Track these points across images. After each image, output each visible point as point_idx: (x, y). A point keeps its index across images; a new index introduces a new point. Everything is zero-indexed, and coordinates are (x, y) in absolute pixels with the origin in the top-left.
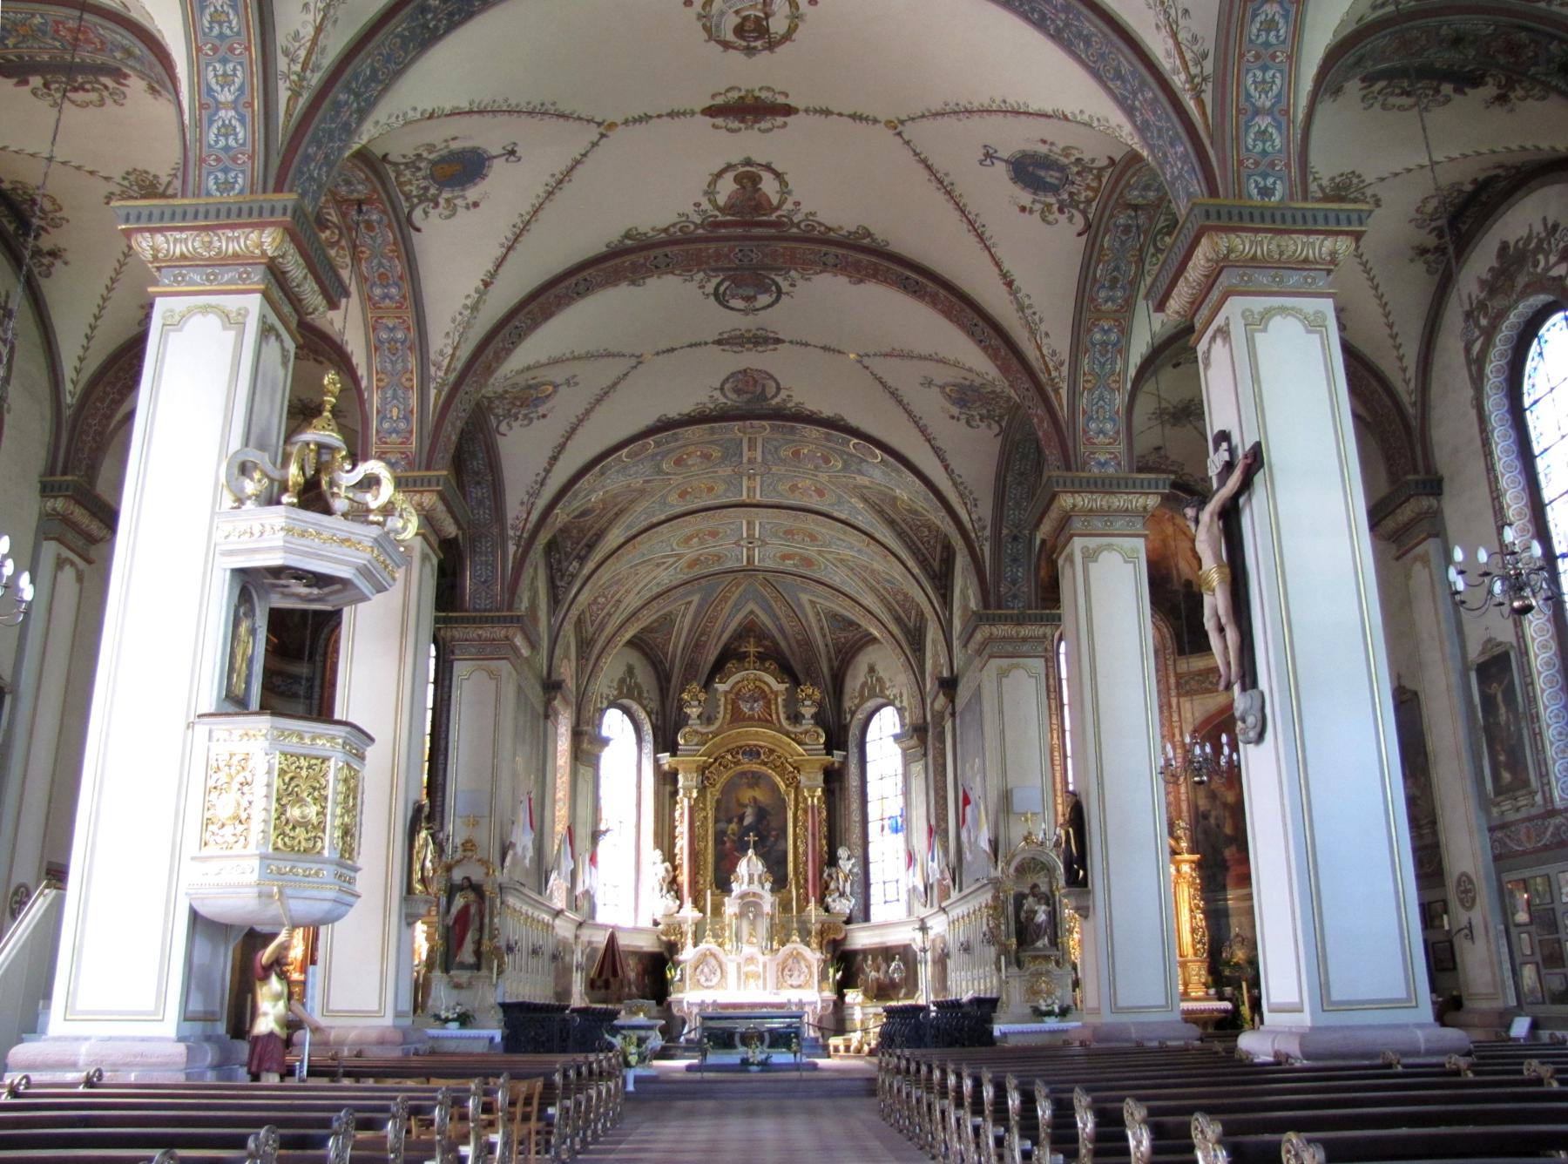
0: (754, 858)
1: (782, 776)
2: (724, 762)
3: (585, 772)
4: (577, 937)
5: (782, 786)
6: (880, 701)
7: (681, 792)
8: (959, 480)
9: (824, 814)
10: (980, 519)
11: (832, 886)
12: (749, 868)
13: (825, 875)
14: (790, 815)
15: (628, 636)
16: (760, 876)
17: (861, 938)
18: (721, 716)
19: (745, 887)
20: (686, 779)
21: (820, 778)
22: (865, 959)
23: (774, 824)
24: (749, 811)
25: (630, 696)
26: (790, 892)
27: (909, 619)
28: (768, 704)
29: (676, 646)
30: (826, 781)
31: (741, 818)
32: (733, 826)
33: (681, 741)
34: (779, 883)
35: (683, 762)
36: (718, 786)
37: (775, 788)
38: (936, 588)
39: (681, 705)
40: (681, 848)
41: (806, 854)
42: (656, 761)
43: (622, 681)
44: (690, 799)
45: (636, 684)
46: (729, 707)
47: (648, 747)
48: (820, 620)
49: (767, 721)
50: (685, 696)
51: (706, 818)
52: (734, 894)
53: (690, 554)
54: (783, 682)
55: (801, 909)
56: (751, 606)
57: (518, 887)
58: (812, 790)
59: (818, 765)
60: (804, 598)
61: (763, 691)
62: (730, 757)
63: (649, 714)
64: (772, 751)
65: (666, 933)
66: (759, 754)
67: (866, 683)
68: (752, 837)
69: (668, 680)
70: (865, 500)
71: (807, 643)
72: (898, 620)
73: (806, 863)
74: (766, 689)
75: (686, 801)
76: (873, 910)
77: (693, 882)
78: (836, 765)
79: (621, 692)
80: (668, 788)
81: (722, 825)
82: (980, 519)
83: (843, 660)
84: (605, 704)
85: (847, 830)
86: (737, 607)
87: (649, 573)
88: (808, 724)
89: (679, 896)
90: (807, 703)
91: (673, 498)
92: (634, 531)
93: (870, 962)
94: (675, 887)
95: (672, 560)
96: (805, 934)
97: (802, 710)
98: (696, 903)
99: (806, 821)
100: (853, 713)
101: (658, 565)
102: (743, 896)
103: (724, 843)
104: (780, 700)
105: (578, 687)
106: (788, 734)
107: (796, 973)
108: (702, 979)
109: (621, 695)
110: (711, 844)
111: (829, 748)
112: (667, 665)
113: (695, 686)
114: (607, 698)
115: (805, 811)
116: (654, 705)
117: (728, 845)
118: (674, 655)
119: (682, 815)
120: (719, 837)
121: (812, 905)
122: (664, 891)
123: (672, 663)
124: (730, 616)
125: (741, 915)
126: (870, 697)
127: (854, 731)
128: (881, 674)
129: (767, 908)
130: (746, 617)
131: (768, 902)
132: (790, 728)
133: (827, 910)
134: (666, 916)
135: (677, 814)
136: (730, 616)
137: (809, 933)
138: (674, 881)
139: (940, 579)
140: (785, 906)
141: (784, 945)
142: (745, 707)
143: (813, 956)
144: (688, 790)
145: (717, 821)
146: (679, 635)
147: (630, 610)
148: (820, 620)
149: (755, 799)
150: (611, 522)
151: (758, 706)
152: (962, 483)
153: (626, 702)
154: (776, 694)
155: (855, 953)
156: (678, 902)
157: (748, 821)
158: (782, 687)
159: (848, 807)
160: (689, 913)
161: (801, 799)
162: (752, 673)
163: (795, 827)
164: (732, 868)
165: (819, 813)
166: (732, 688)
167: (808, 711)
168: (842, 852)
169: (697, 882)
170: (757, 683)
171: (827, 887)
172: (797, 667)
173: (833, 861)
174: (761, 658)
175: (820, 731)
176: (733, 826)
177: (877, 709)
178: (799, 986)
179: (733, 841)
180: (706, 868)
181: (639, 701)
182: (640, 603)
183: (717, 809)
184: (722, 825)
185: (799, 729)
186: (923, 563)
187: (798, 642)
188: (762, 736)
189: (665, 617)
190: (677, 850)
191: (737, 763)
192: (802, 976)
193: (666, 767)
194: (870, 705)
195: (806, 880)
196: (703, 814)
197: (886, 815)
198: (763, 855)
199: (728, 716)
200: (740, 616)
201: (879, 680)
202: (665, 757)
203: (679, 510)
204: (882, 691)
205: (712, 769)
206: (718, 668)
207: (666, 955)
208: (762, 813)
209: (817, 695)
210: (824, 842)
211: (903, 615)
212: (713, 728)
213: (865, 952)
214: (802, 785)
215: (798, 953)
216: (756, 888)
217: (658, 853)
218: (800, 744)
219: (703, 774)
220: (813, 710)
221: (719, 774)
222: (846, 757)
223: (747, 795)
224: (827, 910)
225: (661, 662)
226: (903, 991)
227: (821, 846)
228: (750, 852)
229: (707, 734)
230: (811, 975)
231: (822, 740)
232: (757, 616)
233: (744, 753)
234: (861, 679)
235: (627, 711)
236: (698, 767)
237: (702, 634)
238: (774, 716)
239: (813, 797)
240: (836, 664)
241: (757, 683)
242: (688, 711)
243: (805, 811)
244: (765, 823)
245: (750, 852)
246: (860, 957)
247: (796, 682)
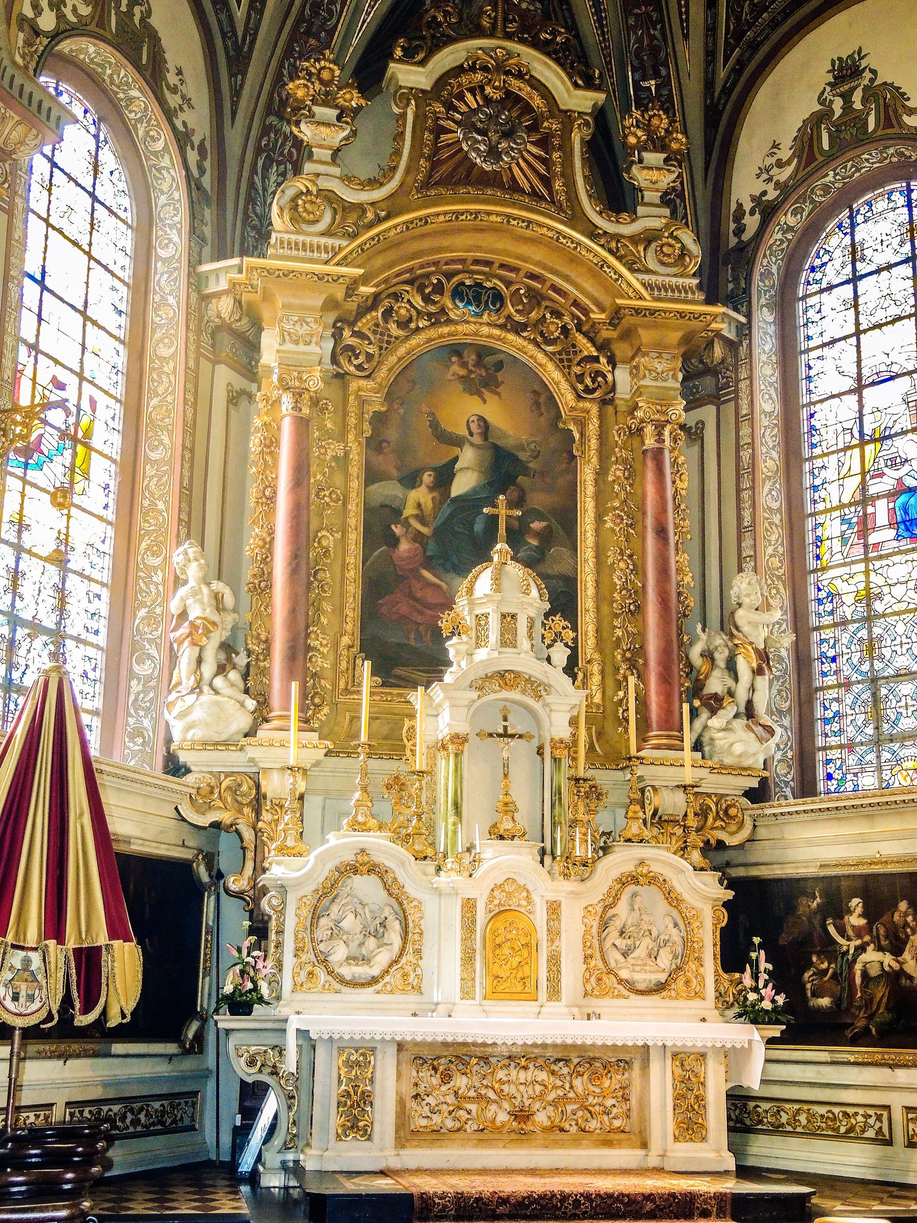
14: (587, 474)
24: (468, 457)
28: (544, 143)
36: (382, 373)
42: (196, 281)
44: (298, 395)
50: (298, 89)
54: (590, 84)
59: (675, 337)
61: (528, 108)
62: (418, 301)
64: (536, 298)
74: (537, 102)
75: (287, 400)
93: (856, 920)
102: (482, 684)
103: (394, 541)
108: (339, 953)
110: (355, 537)
117: (404, 546)
122: (208, 669)
126: (840, 147)
135: (254, 443)
145: (372, 476)
149: (485, 426)
154: (567, 118)
156: (251, 704)
166: (442, 81)
170: (515, 84)
178: (659, 988)
179: (418, 537)
184: (389, 490)
191: (439, 318)
196: (335, 449)
219: (337, 336)
221: (387, 344)
222: (745, 331)
229: (360, 208)
233: (458, 293)
236: (330, 304)
238: (558, 185)
240: (722, 74)
241: (515, 84)
242: (306, 132)
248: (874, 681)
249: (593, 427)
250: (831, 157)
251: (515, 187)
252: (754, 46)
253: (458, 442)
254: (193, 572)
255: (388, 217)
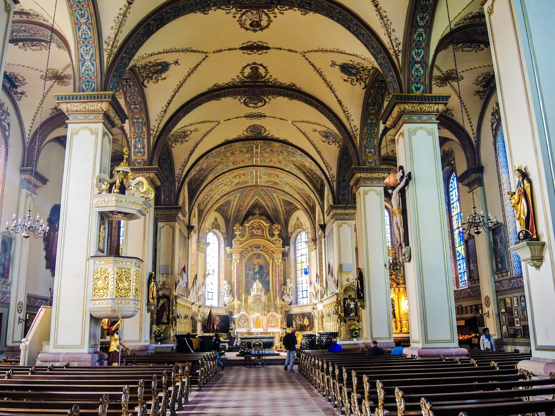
0: (258, 283)
1: (268, 254)
2: (248, 250)
3: (201, 255)
4: (199, 311)
5: (268, 258)
6: (301, 230)
7: (234, 260)
8: (325, 162)
9: (282, 268)
10: (332, 174)
11: (285, 292)
12: (257, 286)
13: (283, 288)
14: (271, 268)
15: (215, 208)
16: (260, 289)
17: (295, 310)
18: (247, 235)
19: (255, 293)
20: (235, 255)
21: (281, 255)
22: (296, 317)
23: (265, 271)
24: (257, 267)
25: (216, 228)
26: (271, 294)
27: (310, 203)
29: (231, 211)
30: (283, 256)
31: (254, 269)
32: (251, 272)
33: (233, 243)
34: (267, 291)
35: (234, 250)
37: (265, 259)
38: (319, 194)
39: (233, 231)
40: (234, 280)
41: (276, 281)
42: (225, 250)
43: (213, 223)
44: (236, 263)
45: (219, 224)
46: (250, 231)
47: (222, 245)
48: (280, 202)
49: (262, 236)
50: (235, 228)
51: (242, 269)
52: (252, 295)
53: (236, 181)
55: (274, 300)
56: (257, 197)
57: (181, 296)
58: (278, 259)
60: (275, 195)
62: (250, 249)
63: (222, 234)
64: (264, 246)
65: (228, 309)
66: (260, 247)
67: (296, 223)
68: (258, 276)
69: (229, 222)
70: (295, 165)
71: (276, 210)
72: (307, 203)
73: (276, 284)
74: (262, 225)
75: (235, 264)
76: (299, 300)
77: (238, 291)
78: (286, 251)
79: (213, 227)
80: (229, 259)
81: (248, 272)
82: (332, 174)
83: (288, 215)
84: (208, 231)
85: (290, 273)
86: (252, 197)
87: (222, 187)
88: (276, 237)
89: (233, 296)
90: (276, 230)
91: (230, 164)
92: (217, 175)
93: (298, 318)
94: (232, 293)
95: (230, 183)
96: (276, 308)
97: (275, 233)
98: (239, 299)
99: (276, 270)
100: (292, 234)
101: (225, 185)
102: (255, 296)
103: (248, 278)
104: (267, 229)
105: (198, 225)
106: (269, 241)
107: (273, 322)
108: (241, 324)
109: (213, 228)
111: (284, 245)
112: (228, 217)
113: (238, 225)
114: (208, 229)
115: (276, 267)
116: (224, 231)
117: (250, 278)
118: (231, 214)
119: (234, 268)
120: (247, 275)
121: (278, 299)
122: (228, 294)
123: (230, 217)
124: (250, 201)
125: (254, 302)
127: (292, 240)
128: (301, 220)
129: (263, 300)
130: (255, 201)
131: (264, 298)
132: (270, 239)
133: (283, 300)
134: (229, 303)
135: (232, 268)
136: (250, 201)
137: (277, 308)
138: (231, 291)
139: (320, 192)
140: (269, 299)
141: (268, 312)
142: (255, 232)
143: (279, 316)
144: (236, 260)
145: (246, 270)
146: (232, 207)
147: (216, 199)
148: (280, 202)
149: (259, 263)
150: (209, 173)
151: (260, 231)
152: (326, 163)
153: (215, 230)
154: (265, 227)
155: (293, 315)
157: (256, 270)
158: (268, 225)
159: (290, 266)
160: (236, 303)
161: (274, 262)
162: (257, 220)
163: (272, 272)
164: (251, 287)
165: (280, 267)
167: (276, 233)
168: (288, 281)
169: (239, 291)
171: (283, 293)
172: (272, 217)
173: (285, 284)
174: (261, 215)
175: (280, 239)
176: (251, 272)
177: (300, 232)
179: (251, 277)
180: (242, 286)
181: (219, 229)
182: (219, 197)
183: (246, 266)
184: (248, 272)
185: (274, 239)
186: (315, 186)
187: (273, 209)
188: (262, 242)
189: (227, 201)
190: (232, 280)
191: (253, 251)
192: (275, 323)
193: (228, 252)
194: (298, 231)
195: (276, 290)
196: (241, 268)
197: (303, 268)
198: (262, 282)
199: (249, 235)
200: (253, 201)
201: (301, 222)
202: (228, 249)
203: (232, 168)
204: (301, 226)
205: (244, 252)
206: (246, 218)
207: (229, 316)
208: (261, 267)
209: (279, 228)
210: (282, 277)
211: (308, 201)
212: (244, 239)
213: (296, 315)
214: (274, 258)
215: (274, 315)
216: (259, 293)
217: (226, 281)
218: (274, 244)
219: (241, 254)
220: (278, 232)
221: (247, 254)
222: (289, 249)
223: (256, 261)
224: (283, 300)
225: (226, 216)
226: (309, 328)
227: (281, 279)
228: (257, 281)
230: (278, 322)
231: (281, 243)
232: (259, 201)
233: (255, 247)
234: (294, 222)
235: (215, 233)
237: (240, 207)
239: (278, 262)
240: (286, 217)
242: (236, 233)
243: (276, 267)
244: (262, 271)
245: (257, 281)
246: (294, 316)
247: (273, 223)
248: (302, 291)
249: (271, 262)
250: (297, 229)
251: (260, 236)
252: (289, 213)
253: (255, 265)
254: (226, 284)
255: (246, 241)
